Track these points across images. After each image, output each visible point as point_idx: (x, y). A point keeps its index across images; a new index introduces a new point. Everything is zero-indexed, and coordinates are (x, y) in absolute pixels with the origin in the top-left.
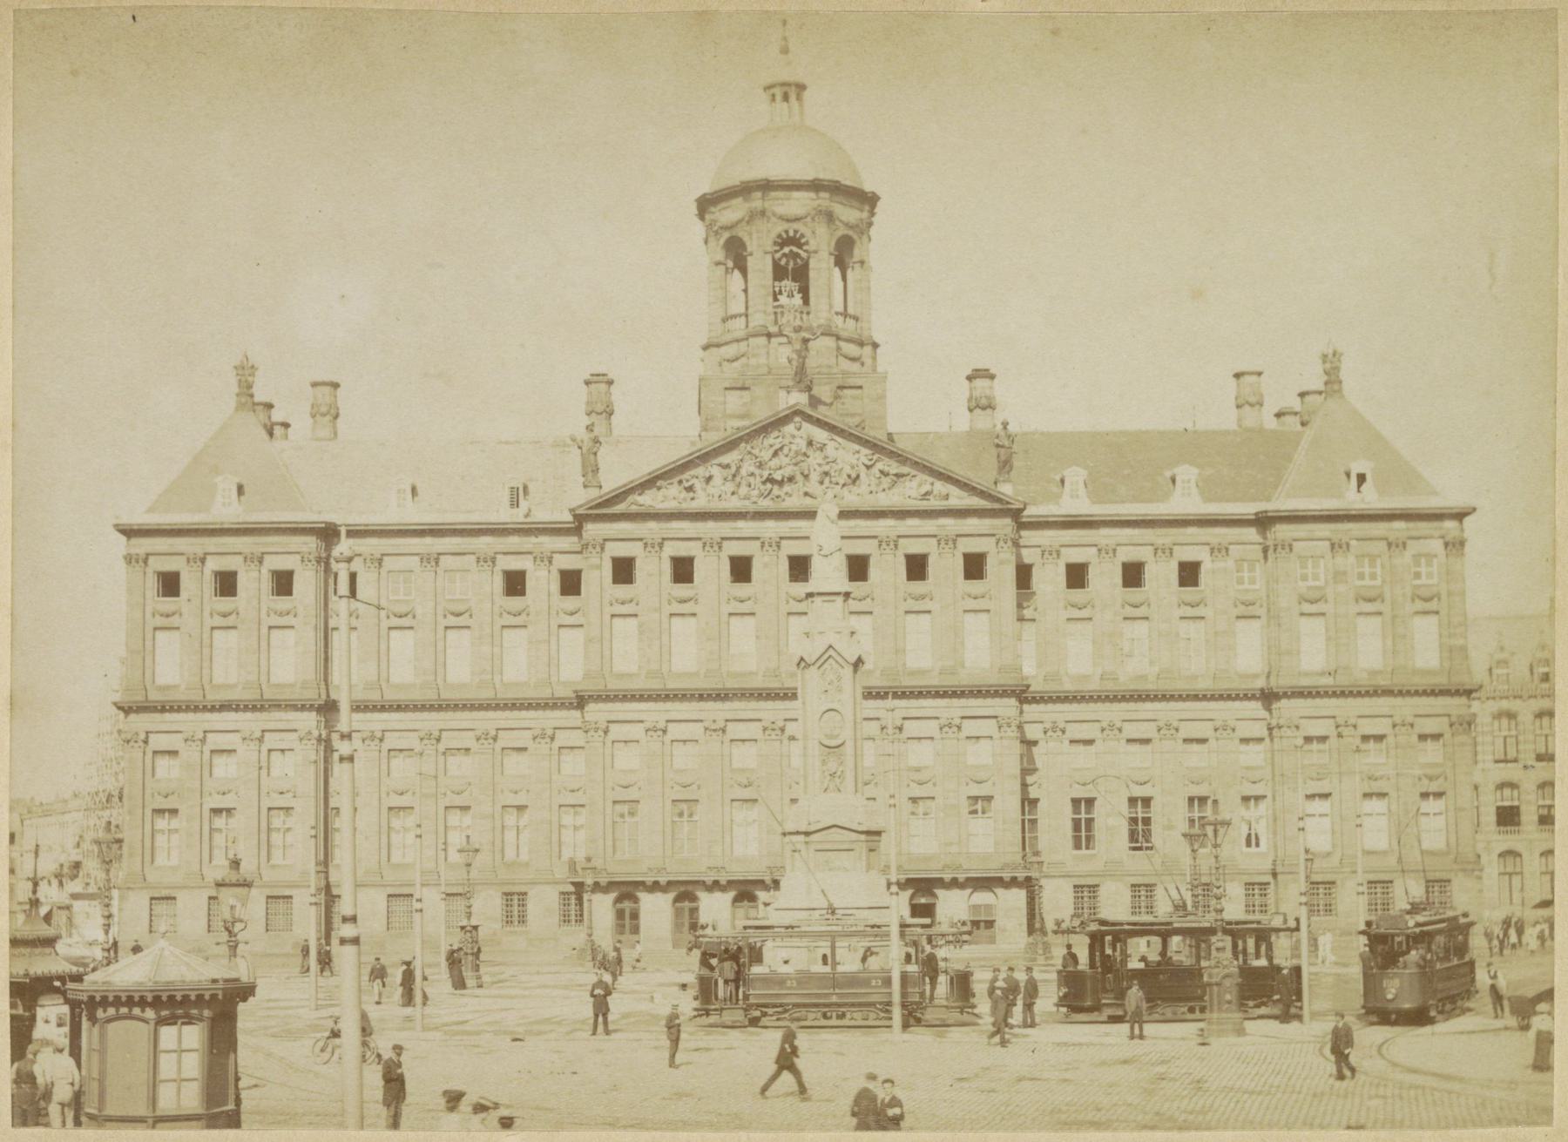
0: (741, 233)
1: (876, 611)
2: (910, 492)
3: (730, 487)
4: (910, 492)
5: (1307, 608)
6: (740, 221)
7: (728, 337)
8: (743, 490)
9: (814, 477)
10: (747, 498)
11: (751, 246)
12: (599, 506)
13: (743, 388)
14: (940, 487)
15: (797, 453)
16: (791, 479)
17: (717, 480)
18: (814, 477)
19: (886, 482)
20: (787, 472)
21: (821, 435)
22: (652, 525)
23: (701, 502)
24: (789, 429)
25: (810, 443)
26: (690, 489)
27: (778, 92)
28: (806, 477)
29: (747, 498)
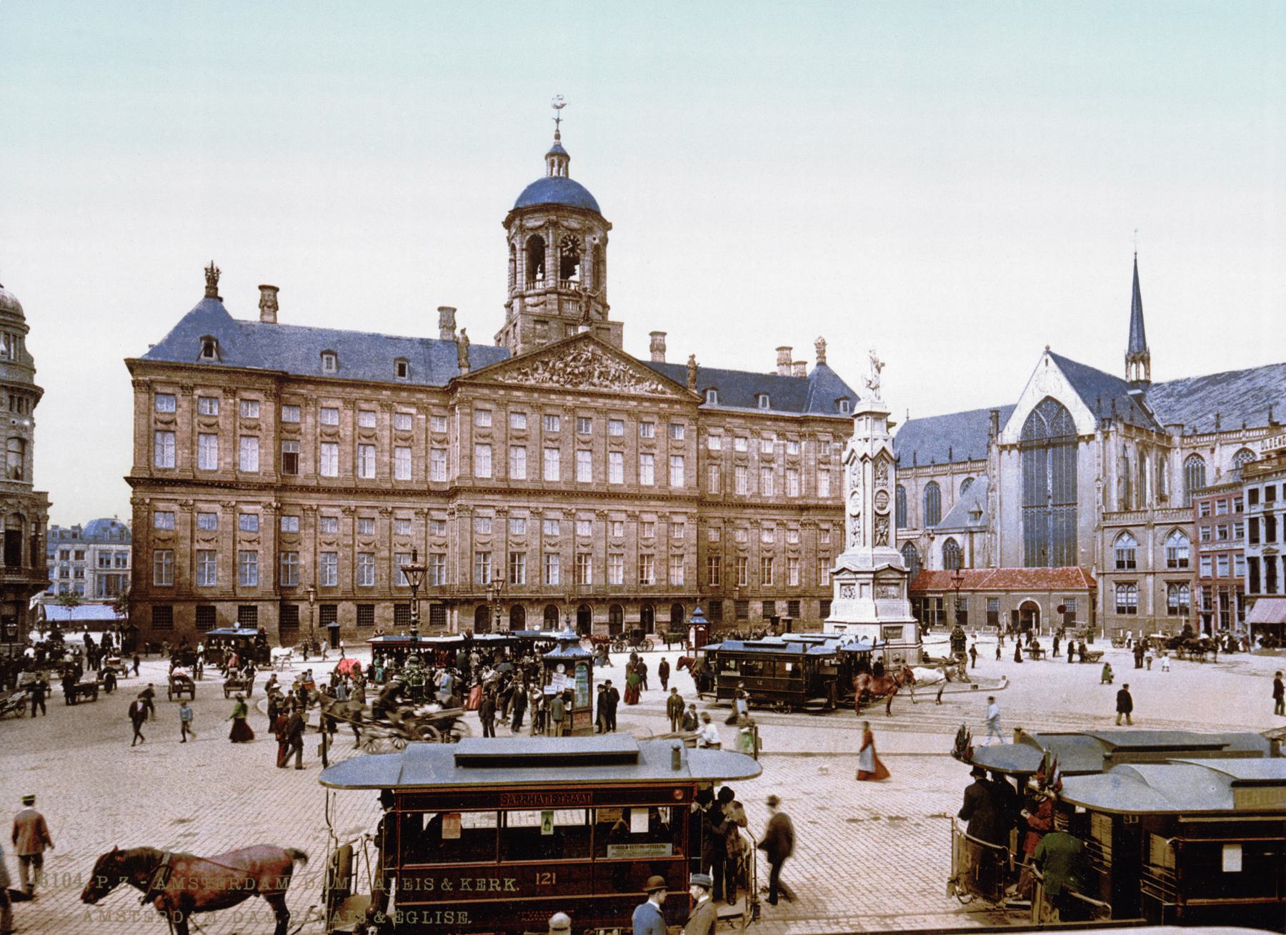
0: (542, 234)
1: (626, 451)
2: (644, 389)
3: (547, 375)
4: (644, 389)
5: (822, 466)
6: (540, 227)
7: (532, 292)
8: (555, 378)
9: (596, 374)
10: (558, 382)
11: (550, 240)
12: (471, 378)
13: (545, 322)
14: (660, 387)
15: (587, 360)
16: (582, 374)
17: (540, 371)
18: (596, 374)
19: (633, 381)
20: (582, 369)
21: (600, 352)
22: (502, 392)
23: (532, 382)
24: (581, 345)
25: (593, 354)
26: (526, 374)
27: (555, 159)
28: (591, 374)
29: (558, 382)
